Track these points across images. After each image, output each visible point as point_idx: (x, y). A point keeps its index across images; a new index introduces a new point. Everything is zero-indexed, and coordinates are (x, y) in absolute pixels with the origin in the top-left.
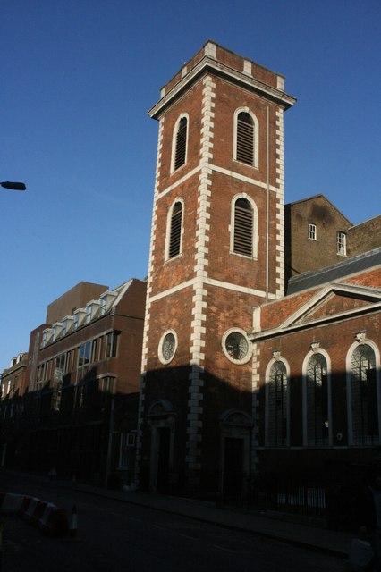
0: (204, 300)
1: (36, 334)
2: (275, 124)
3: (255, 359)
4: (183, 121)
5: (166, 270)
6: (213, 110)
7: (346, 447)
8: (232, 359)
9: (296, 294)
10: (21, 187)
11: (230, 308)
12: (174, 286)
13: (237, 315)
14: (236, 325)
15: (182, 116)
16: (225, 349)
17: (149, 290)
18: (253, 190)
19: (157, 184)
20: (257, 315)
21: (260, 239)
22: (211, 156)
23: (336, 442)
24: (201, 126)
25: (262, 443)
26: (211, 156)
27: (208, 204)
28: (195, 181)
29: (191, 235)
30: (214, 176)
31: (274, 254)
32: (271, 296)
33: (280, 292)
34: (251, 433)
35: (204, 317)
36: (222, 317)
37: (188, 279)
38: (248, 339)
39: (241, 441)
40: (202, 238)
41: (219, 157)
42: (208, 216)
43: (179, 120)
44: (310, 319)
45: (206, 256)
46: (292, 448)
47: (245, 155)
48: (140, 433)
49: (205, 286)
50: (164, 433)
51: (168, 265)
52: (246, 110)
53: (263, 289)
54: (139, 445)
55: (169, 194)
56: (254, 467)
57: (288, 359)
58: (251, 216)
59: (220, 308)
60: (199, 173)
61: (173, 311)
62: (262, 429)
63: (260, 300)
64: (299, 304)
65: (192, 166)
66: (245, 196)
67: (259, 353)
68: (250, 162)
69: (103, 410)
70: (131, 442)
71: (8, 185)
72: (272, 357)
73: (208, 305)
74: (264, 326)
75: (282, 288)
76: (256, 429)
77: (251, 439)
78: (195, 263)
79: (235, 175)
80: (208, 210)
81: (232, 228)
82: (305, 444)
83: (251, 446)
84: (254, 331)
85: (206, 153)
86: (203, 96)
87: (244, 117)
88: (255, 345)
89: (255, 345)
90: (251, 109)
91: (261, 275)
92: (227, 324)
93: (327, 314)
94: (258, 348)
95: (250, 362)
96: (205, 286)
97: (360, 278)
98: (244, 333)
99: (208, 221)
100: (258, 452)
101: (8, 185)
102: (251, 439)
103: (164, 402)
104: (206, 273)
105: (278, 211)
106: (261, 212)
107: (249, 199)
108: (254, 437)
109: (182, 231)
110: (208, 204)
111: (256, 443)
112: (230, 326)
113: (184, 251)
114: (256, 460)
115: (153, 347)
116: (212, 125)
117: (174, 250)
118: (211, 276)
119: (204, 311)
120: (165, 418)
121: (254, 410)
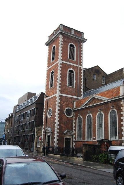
1: (15, 108)
2: (81, 47)
3: (74, 116)
4: (54, 47)
5: (49, 91)
6: (62, 44)
7: (95, 141)
8: (67, 116)
12: (52, 95)
14: (68, 107)
15: (54, 46)
16: (65, 114)
18: (74, 67)
20: (75, 103)
21: (76, 81)
22: (61, 58)
23: (93, 139)
24: (59, 49)
25: (75, 140)
26: (61, 58)
27: (61, 72)
28: (57, 65)
29: (56, 81)
30: (62, 64)
31: (80, 85)
32: (79, 98)
36: (64, 105)
39: (70, 139)
40: (59, 82)
41: (64, 58)
42: (61, 76)
46: (83, 141)
47: (72, 57)
48: (43, 137)
49: (60, 96)
50: (49, 137)
52: (72, 44)
54: (42, 140)
56: (73, 146)
58: (73, 75)
59: (64, 102)
60: (58, 63)
62: (76, 136)
65: (57, 61)
66: (72, 69)
70: (40, 140)
72: (78, 116)
73: (60, 101)
74: (77, 107)
75: (83, 95)
77: (73, 139)
78: (57, 89)
79: (69, 63)
80: (61, 74)
81: (67, 79)
82: (86, 140)
83: (73, 141)
84: (74, 108)
85: (60, 57)
86: (59, 40)
90: (73, 43)
91: (76, 92)
94: (75, 113)
95: (73, 117)
96: (60, 96)
98: (71, 109)
99: (60, 77)
102: (73, 139)
105: (82, 73)
107: (73, 70)
109: (54, 80)
110: (61, 72)
111: (74, 139)
112: (67, 107)
114: (74, 144)
116: (62, 49)
117: (52, 85)
118: (61, 93)
119: (59, 103)
120: (49, 133)
121: (74, 130)
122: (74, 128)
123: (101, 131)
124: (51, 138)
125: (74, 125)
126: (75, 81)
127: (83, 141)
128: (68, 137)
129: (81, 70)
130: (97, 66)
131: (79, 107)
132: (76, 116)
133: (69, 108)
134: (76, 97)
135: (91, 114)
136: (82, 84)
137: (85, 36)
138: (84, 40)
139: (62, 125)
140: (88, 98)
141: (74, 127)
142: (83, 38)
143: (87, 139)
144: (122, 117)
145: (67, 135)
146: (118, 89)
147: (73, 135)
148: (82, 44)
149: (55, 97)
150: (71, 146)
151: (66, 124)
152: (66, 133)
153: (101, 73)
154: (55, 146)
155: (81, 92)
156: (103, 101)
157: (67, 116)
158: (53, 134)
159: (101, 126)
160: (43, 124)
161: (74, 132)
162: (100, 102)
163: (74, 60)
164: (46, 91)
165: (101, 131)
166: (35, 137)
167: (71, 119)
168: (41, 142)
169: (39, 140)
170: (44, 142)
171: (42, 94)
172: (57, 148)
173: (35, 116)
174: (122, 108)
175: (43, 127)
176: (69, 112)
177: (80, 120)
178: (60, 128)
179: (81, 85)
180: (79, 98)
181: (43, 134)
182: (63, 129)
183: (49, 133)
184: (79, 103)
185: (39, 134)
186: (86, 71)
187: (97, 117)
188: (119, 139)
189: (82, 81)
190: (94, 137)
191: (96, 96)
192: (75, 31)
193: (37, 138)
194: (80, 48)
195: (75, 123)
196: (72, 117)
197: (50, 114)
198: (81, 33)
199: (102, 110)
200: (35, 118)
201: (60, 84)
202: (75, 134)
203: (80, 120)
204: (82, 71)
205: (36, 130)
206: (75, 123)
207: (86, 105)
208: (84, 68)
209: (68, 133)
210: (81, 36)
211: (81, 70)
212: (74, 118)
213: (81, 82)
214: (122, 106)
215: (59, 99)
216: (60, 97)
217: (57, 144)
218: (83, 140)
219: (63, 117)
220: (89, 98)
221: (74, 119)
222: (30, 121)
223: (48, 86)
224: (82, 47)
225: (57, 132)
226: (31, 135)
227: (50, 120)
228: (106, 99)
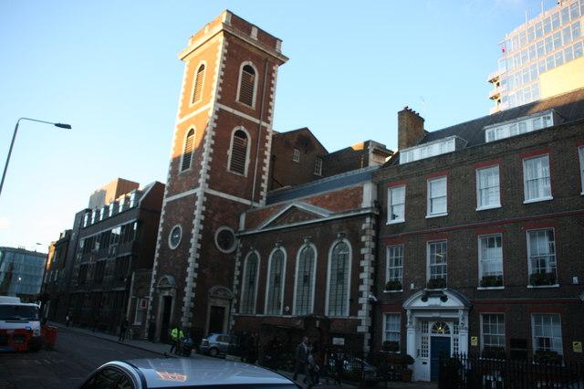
1: (79, 216)
2: (271, 75)
5: (179, 179)
8: (221, 250)
10: (68, 127)
12: (184, 191)
14: (227, 225)
17: (166, 193)
18: (249, 124)
19: (179, 111)
20: (243, 218)
23: (285, 312)
25: (237, 311)
31: (261, 173)
32: (256, 205)
33: (262, 202)
34: (231, 304)
36: (216, 219)
38: (235, 235)
39: (224, 308)
43: (200, 66)
44: (276, 225)
45: (208, 172)
47: (246, 97)
48: (151, 299)
49: (206, 194)
50: (168, 300)
52: (251, 63)
53: (249, 199)
54: (150, 308)
60: (209, 109)
61: (182, 210)
62: (238, 302)
63: (247, 207)
66: (243, 128)
67: (241, 246)
74: (248, 226)
75: (264, 199)
76: (235, 301)
78: (199, 176)
79: (236, 112)
81: (230, 153)
95: (235, 253)
96: (206, 194)
97: (312, 199)
98: (232, 230)
99: (212, 146)
100: (235, 317)
103: (168, 277)
104: (207, 185)
108: (233, 306)
111: (234, 310)
112: (222, 225)
114: (233, 323)
115: (165, 235)
118: (210, 187)
120: (169, 288)
121: (235, 287)
122: (236, 282)
123: (306, 293)
124: (173, 302)
125: (237, 273)
126: (248, 161)
128: (219, 303)
129: (268, 134)
130: (306, 129)
131: (255, 227)
132: (245, 251)
133: (227, 228)
135: (283, 249)
136: (266, 169)
137: (285, 49)
138: (282, 60)
139: (204, 271)
141: (236, 278)
142: (279, 54)
143: (268, 310)
145: (216, 298)
146: (358, 195)
147: (231, 300)
148: (274, 68)
149: (194, 197)
151: (216, 268)
152: (216, 292)
155: (262, 189)
156: (317, 217)
157: (221, 250)
158: (181, 293)
159: (306, 279)
160: (156, 264)
161: (236, 292)
162: (310, 219)
163: (251, 105)
164: (169, 180)
165: (306, 293)
166: (130, 299)
168: (145, 311)
169: (139, 306)
170: (153, 312)
171: (158, 187)
173: (134, 243)
174: (363, 239)
175: (154, 272)
176: (226, 239)
177: (253, 261)
179: (264, 173)
180: (256, 205)
183: (169, 288)
184: (254, 218)
186: (278, 138)
187: (298, 258)
188: (351, 315)
189: (267, 161)
190: (288, 308)
191: (301, 205)
192: (260, 32)
195: (241, 269)
196: (231, 254)
197: (174, 241)
198: (272, 41)
199: (312, 241)
201: (210, 164)
202: (238, 297)
203: (253, 261)
204: (269, 138)
205: (133, 279)
206: (242, 268)
207: (274, 223)
208: (274, 131)
210: (274, 47)
211: (268, 134)
212: (239, 254)
213: (265, 165)
214: (364, 233)
215: (204, 204)
217: (190, 320)
220: (281, 207)
222: (120, 256)
223: (178, 166)
224: (273, 75)
228: (325, 215)
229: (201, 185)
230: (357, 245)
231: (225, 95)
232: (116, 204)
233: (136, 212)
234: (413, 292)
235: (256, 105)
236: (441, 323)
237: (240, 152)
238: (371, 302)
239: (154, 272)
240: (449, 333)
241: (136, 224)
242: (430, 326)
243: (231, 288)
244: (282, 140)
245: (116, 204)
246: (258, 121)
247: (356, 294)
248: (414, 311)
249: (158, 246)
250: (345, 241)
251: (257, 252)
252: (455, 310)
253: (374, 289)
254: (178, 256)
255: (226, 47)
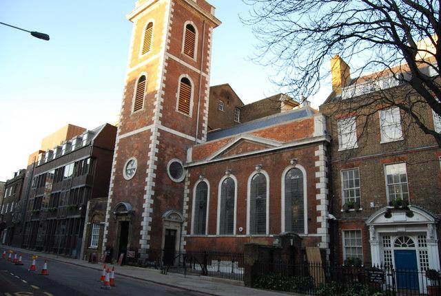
0: (157, 139)
3: (187, 179)
8: (172, 179)
9: (217, 140)
10: (45, 37)
11: (173, 146)
12: (137, 129)
13: (177, 151)
14: (176, 157)
17: (119, 131)
18: (192, 74)
19: (129, 62)
20: (190, 152)
21: (194, 104)
22: (168, 48)
23: (238, 232)
31: (202, 115)
32: (199, 141)
33: (204, 139)
35: (157, 150)
37: (147, 125)
39: (175, 231)
44: (225, 156)
46: (209, 236)
48: (107, 224)
49: (159, 130)
51: (134, 115)
52: (192, 23)
53: (195, 136)
55: (138, 70)
56: (182, 247)
57: (209, 181)
61: (135, 146)
63: (192, 143)
64: (217, 147)
65: (155, 53)
66: (187, 76)
68: (192, 55)
69: (80, 208)
71: (35, 34)
72: (198, 179)
74: (194, 159)
75: (206, 136)
76: (185, 224)
79: (182, 62)
81: (178, 95)
84: (187, 162)
87: (189, 27)
88: (187, 171)
89: (187, 171)
92: (171, 157)
93: (237, 153)
95: (184, 182)
96: (159, 130)
98: (181, 163)
100: (186, 238)
101: (35, 34)
104: (160, 122)
106: (197, 88)
108: (183, 228)
111: (185, 232)
113: (145, 107)
114: (185, 243)
115: (119, 169)
118: (163, 124)
122: (186, 207)
125: (186, 199)
127: (209, 236)
128: (172, 227)
130: (228, 85)
131: (205, 158)
132: (193, 180)
133: (177, 160)
134: (192, 139)
135: (232, 176)
136: (206, 111)
137: (217, 14)
139: (159, 198)
140: (228, 140)
144: (317, 184)
147: (181, 223)
149: (149, 133)
150: (177, 248)
151: (167, 195)
152: (169, 217)
153: (233, 100)
154: (142, 246)
156: (266, 146)
157: (172, 179)
160: (111, 193)
161: (186, 215)
166: (85, 226)
167: (179, 185)
172: (148, 251)
173: (88, 176)
175: (110, 201)
178: (156, 206)
180: (199, 141)
181: (108, 216)
182: (163, 207)
185: (96, 218)
187: (249, 183)
189: (207, 105)
191: (248, 136)
193: (90, 227)
194: (206, 36)
195: (190, 195)
200: (89, 179)
202: (189, 220)
205: (88, 207)
206: (190, 195)
209: (173, 218)
212: (188, 183)
213: (205, 108)
216: (161, 134)
217: (149, 242)
218: (209, 233)
219: (163, 180)
221: (186, 187)
222: (75, 188)
223: (130, 107)
224: (209, 35)
225: (149, 214)
226: (73, 219)
227: (131, 184)
228: (278, 145)
229: (155, 121)
230: (312, 169)
231: (173, 48)
232: (69, 144)
233: (90, 150)
234: (374, 210)
235: (198, 58)
236: (404, 238)
237: (185, 95)
238: (329, 221)
239: (110, 201)
240: (414, 246)
241: (89, 160)
242: (393, 240)
243: (181, 210)
244: (214, 90)
245: (69, 144)
246: (199, 71)
247: (314, 214)
248: (376, 227)
249: (112, 178)
250: (299, 166)
251: (206, 181)
252: (425, 225)
253: (331, 209)
254: (134, 184)
255: (173, 7)
